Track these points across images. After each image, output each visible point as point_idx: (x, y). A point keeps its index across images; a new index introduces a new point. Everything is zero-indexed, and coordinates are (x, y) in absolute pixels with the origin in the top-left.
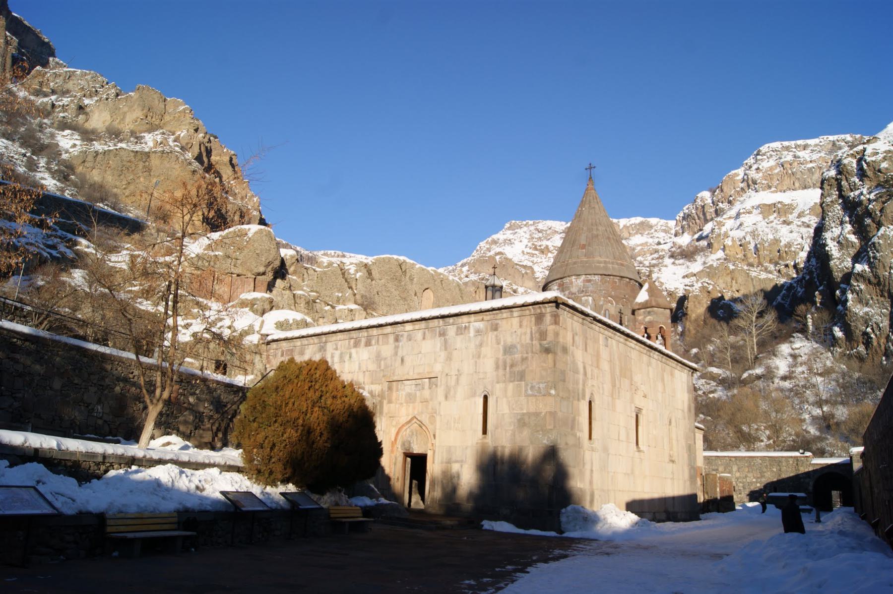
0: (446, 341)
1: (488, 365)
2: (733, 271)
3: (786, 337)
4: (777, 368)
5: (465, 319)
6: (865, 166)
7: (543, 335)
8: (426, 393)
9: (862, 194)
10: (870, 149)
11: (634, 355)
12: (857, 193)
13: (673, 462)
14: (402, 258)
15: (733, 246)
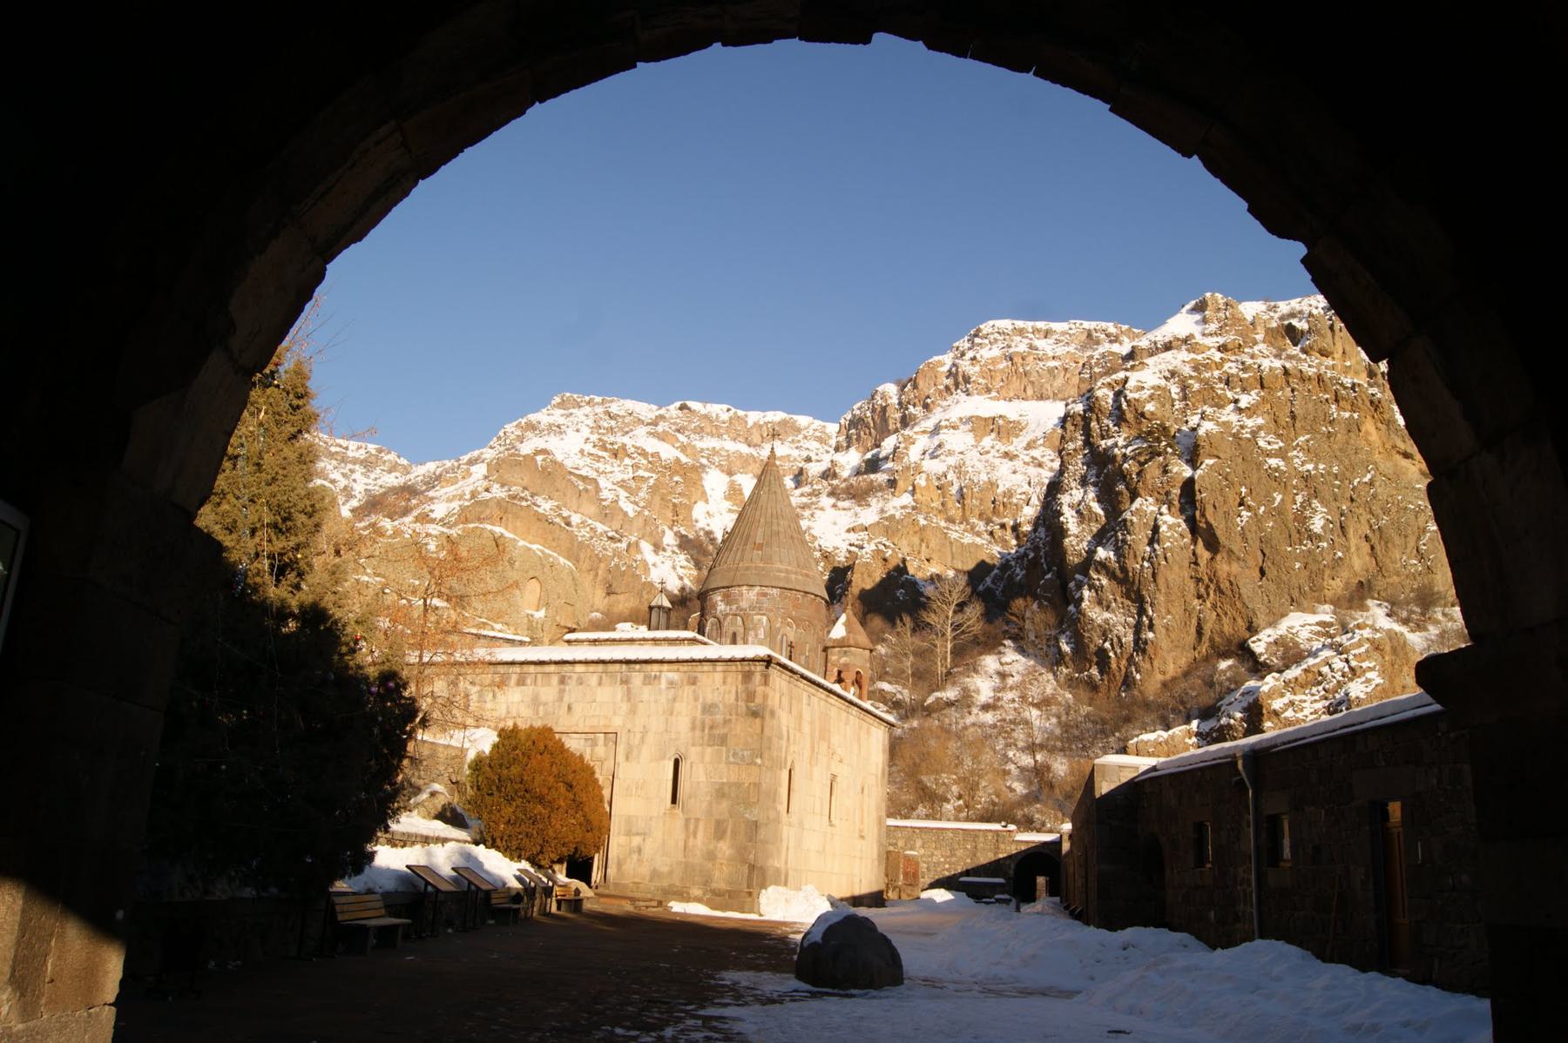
0: (629, 690)
1: (682, 724)
2: (923, 528)
3: (990, 644)
4: (978, 691)
5: (656, 667)
6: (1124, 406)
7: (750, 696)
8: (600, 750)
9: (1116, 445)
10: (1134, 378)
11: (833, 712)
12: (1110, 442)
13: (862, 837)
14: (498, 530)
15: (927, 487)
